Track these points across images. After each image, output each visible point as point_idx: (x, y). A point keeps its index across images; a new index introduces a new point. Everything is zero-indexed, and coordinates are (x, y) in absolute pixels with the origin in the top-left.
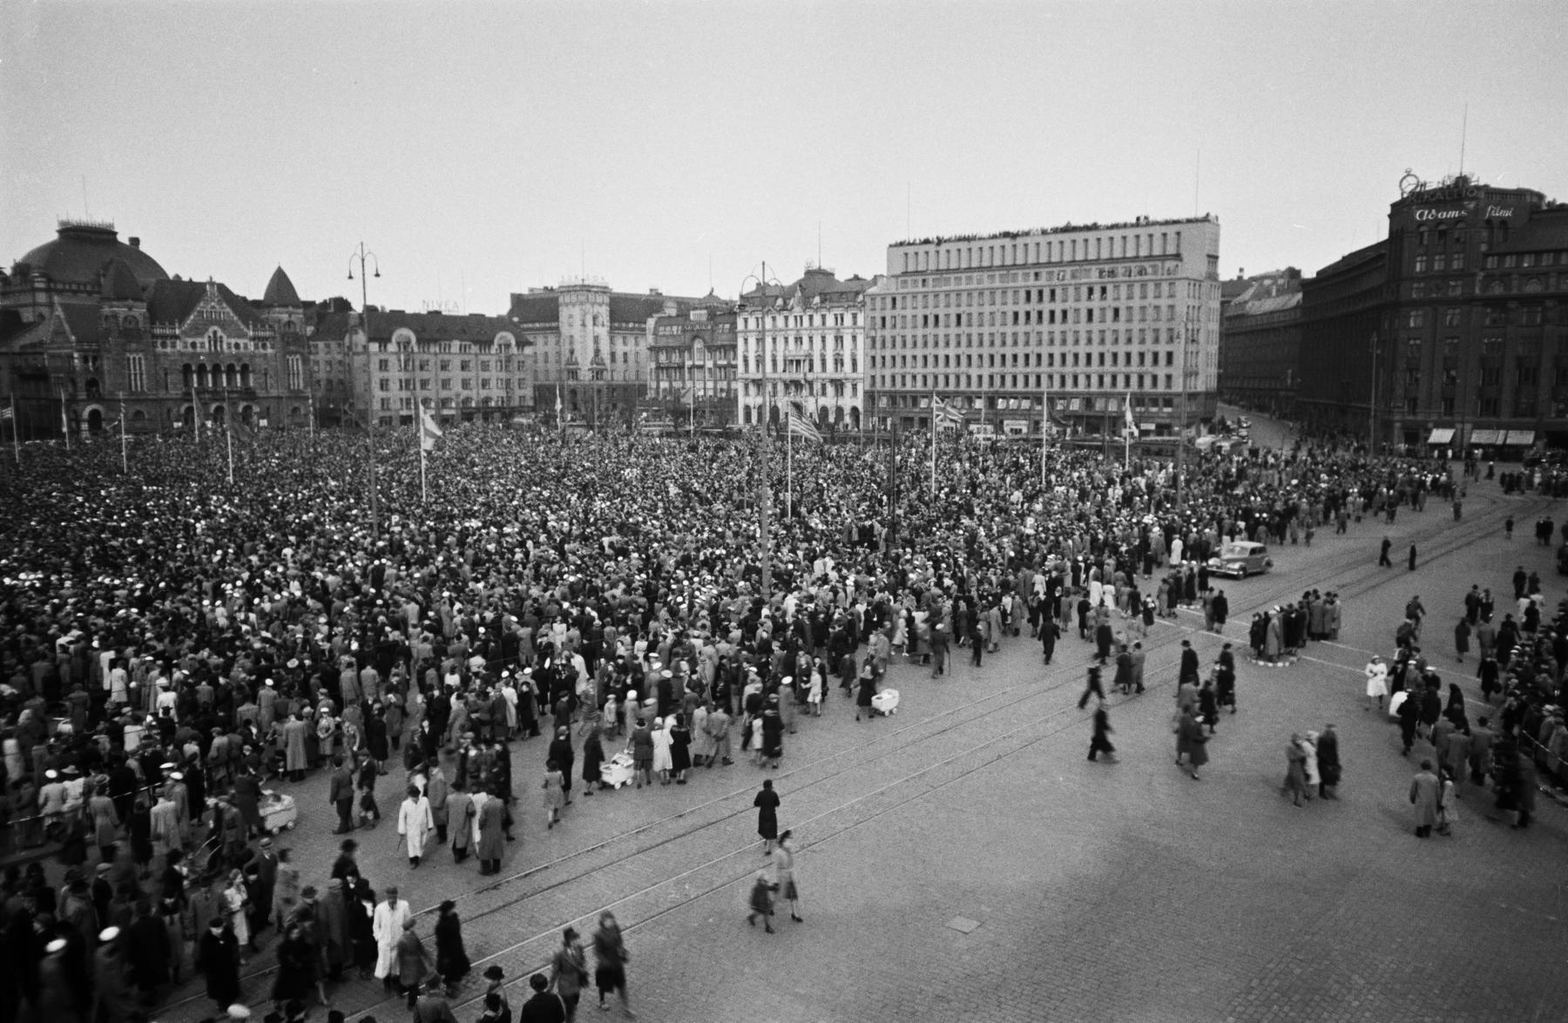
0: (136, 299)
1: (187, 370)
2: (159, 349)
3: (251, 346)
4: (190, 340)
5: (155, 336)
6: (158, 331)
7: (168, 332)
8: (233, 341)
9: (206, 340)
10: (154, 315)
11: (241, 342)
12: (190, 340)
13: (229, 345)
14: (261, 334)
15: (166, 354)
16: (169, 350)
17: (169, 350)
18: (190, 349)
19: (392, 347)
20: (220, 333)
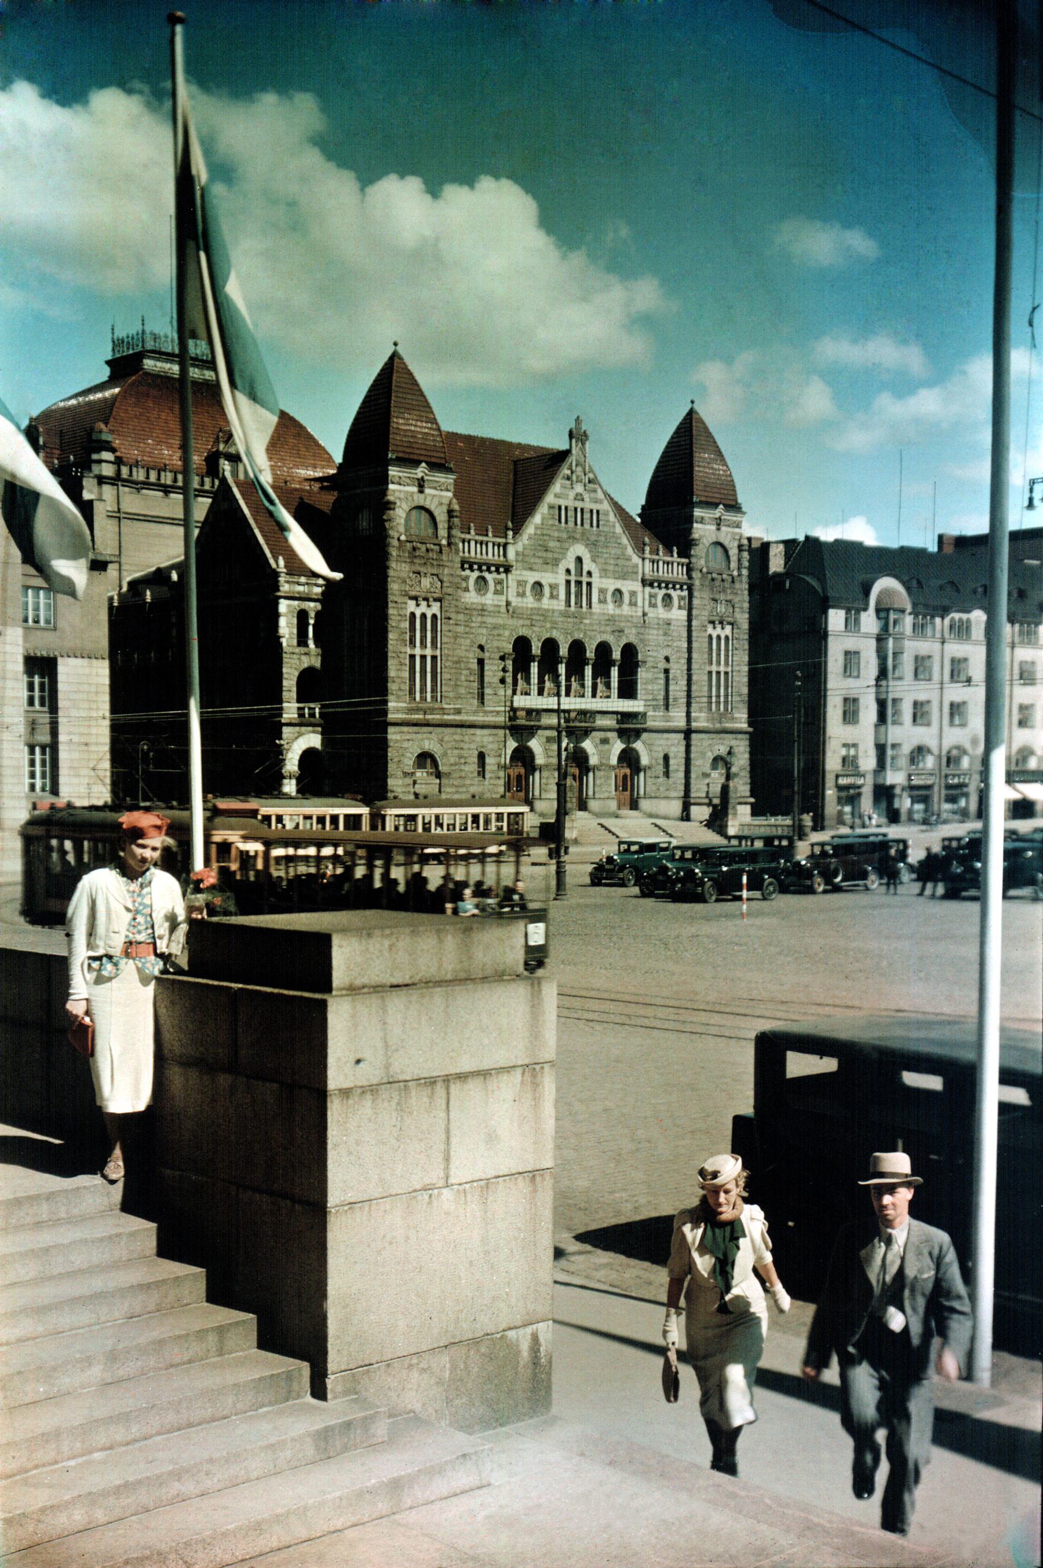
0: (434, 466)
1: (522, 644)
2: (472, 597)
3: (644, 594)
4: (531, 577)
5: (467, 564)
6: (474, 552)
7: (492, 555)
8: (611, 584)
9: (561, 579)
10: (469, 514)
11: (629, 586)
12: (531, 577)
13: (602, 591)
14: (663, 573)
15: (483, 610)
16: (489, 599)
17: (489, 599)
18: (529, 601)
19: (869, 621)
20: (588, 565)
